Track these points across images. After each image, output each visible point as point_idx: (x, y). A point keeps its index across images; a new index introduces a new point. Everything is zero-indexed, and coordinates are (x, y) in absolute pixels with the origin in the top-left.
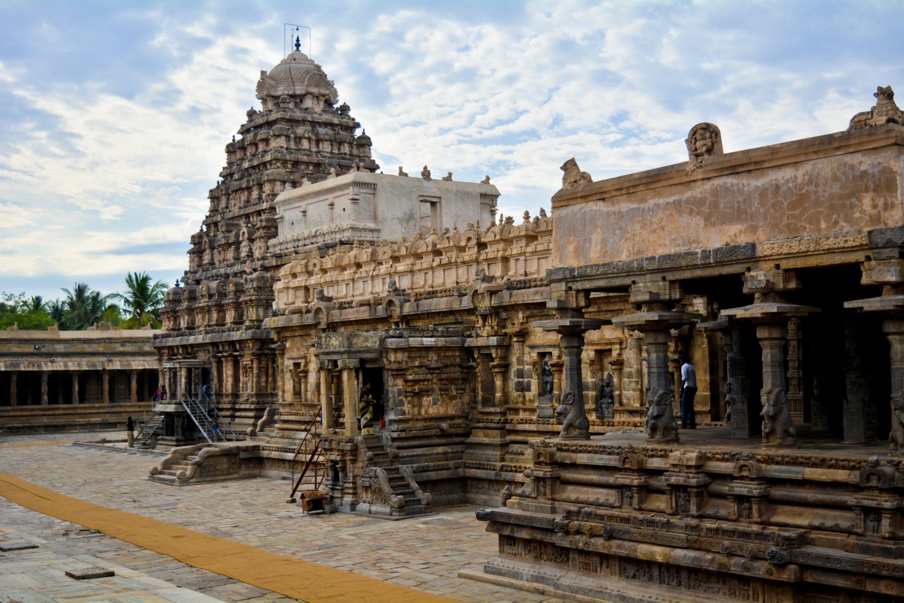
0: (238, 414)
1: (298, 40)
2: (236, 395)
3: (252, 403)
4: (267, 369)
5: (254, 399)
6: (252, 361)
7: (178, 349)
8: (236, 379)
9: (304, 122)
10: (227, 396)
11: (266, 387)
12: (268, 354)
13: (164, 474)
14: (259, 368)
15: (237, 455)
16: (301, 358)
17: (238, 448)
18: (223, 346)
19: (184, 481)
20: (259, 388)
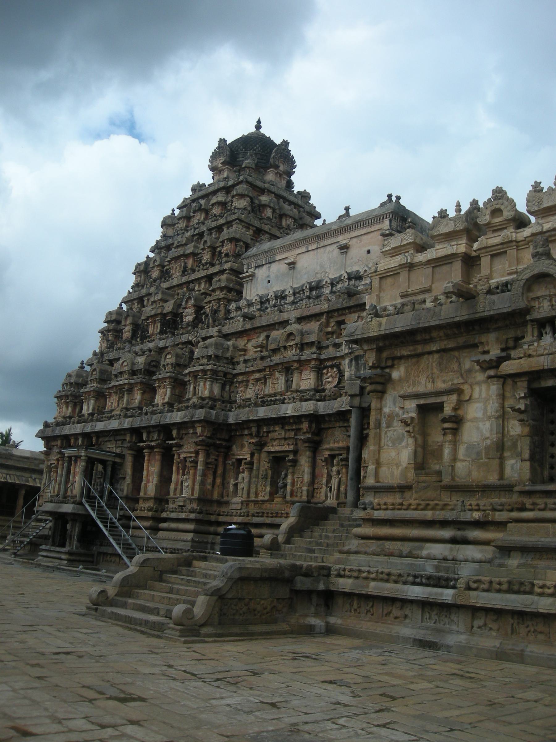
0: (162, 525)
1: (259, 122)
2: (161, 500)
3: (192, 511)
4: (217, 466)
5: (195, 506)
6: (197, 453)
7: (76, 439)
8: (165, 479)
9: (270, 192)
10: (146, 499)
11: (212, 491)
12: (220, 446)
13: (124, 605)
14: (206, 464)
15: (290, 581)
16: (449, 392)
17: (296, 570)
18: (149, 433)
19: (191, 630)
20: (201, 491)
